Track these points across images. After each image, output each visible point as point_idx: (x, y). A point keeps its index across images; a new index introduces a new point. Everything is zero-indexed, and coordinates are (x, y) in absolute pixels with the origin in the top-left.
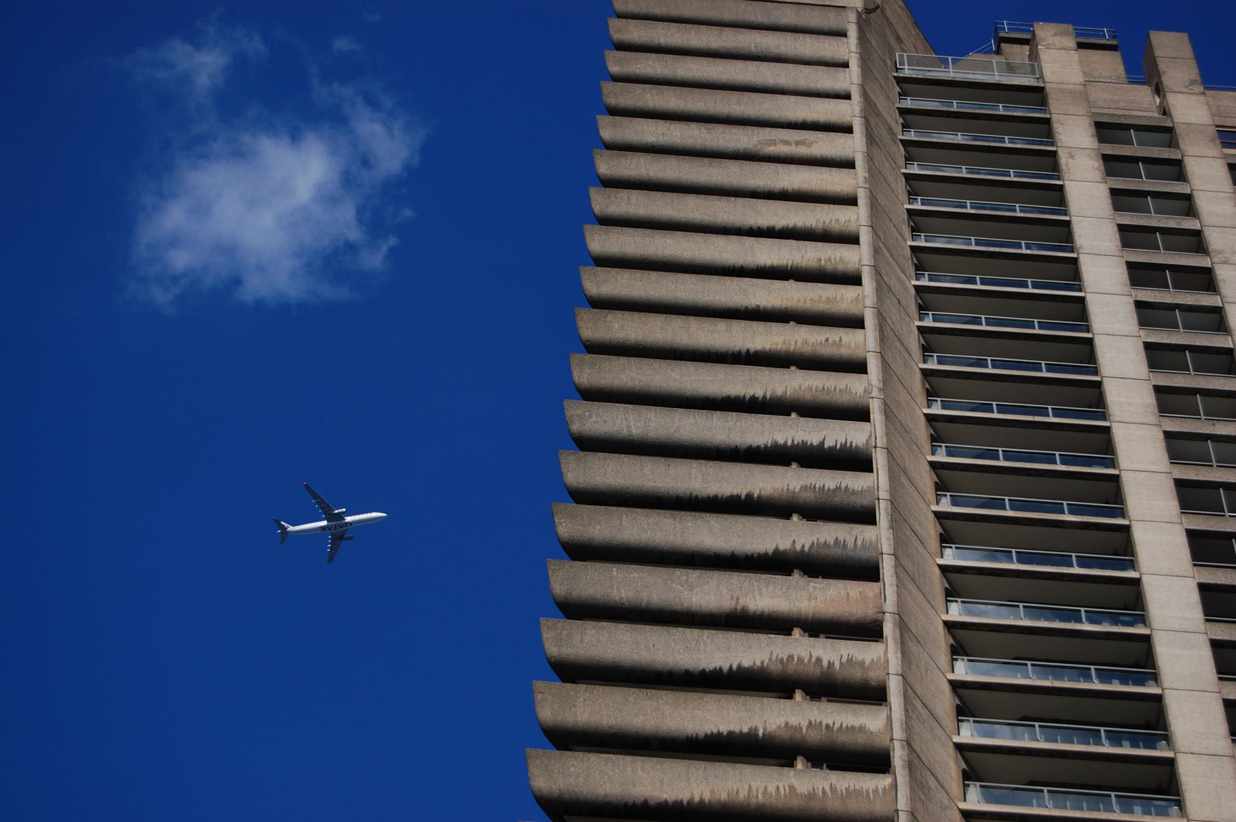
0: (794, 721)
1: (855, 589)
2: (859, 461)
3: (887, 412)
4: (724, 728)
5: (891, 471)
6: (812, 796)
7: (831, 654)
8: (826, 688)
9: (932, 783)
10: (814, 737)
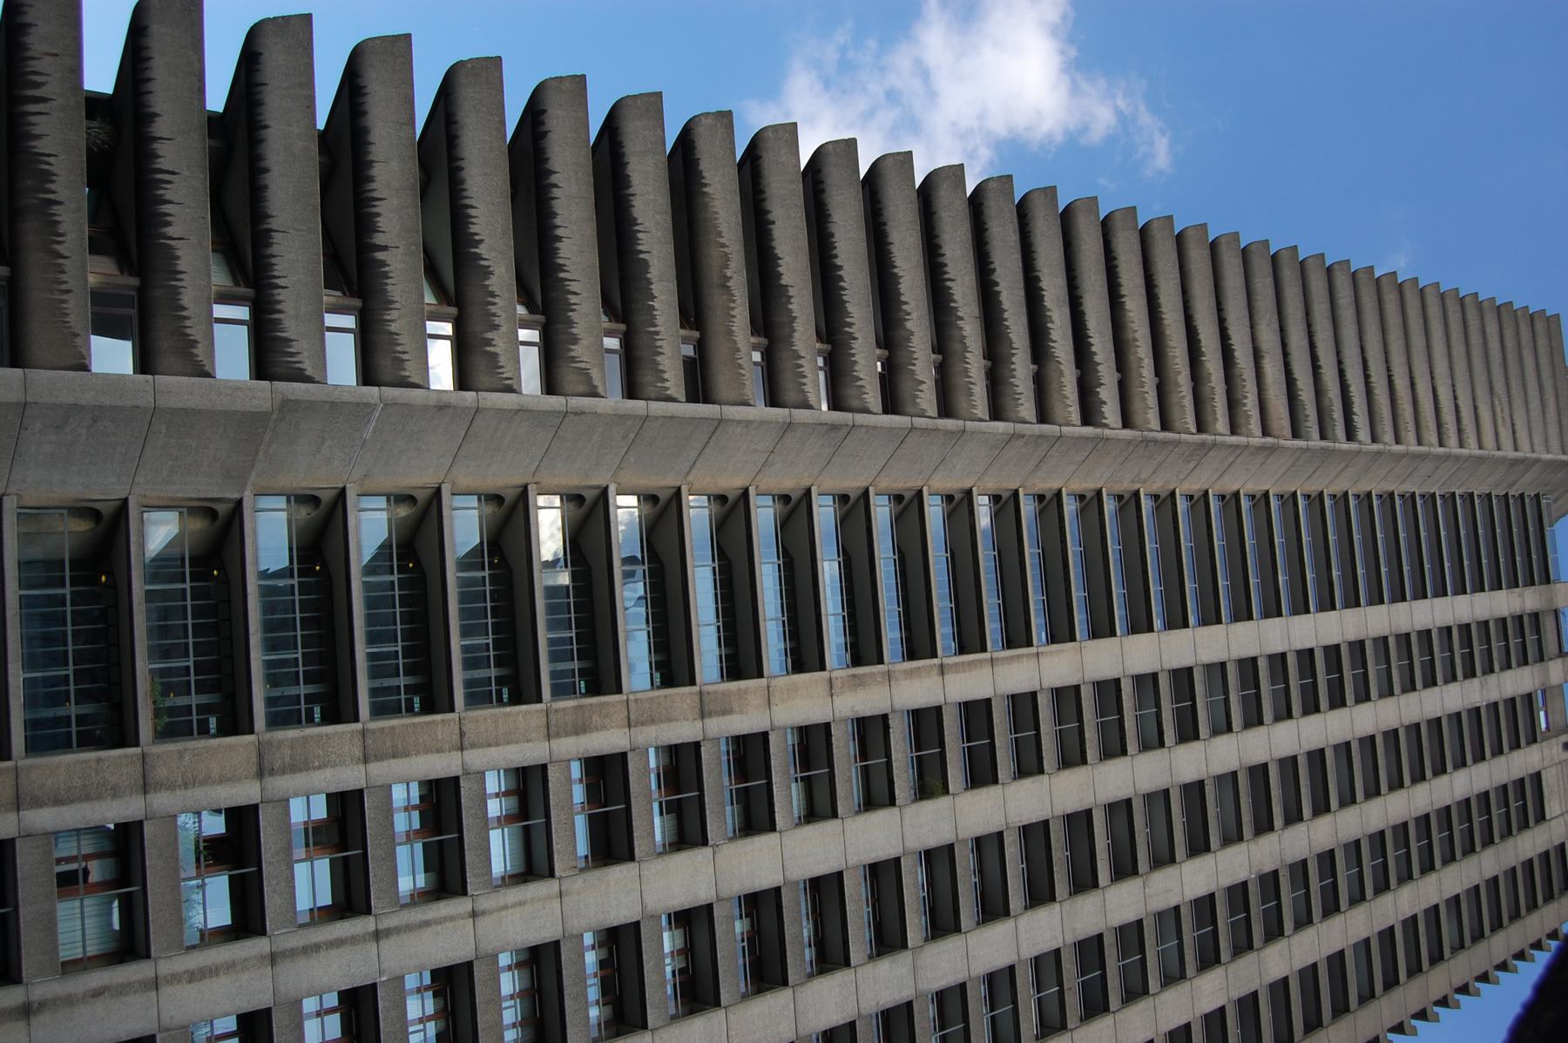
0: (1213, 378)
1: (1286, 423)
2: (1350, 435)
3: (1379, 453)
4: (1201, 337)
5: (1348, 452)
6: (1177, 385)
7: (1250, 404)
8: (1233, 404)
9: (1192, 465)
10: (1206, 390)
